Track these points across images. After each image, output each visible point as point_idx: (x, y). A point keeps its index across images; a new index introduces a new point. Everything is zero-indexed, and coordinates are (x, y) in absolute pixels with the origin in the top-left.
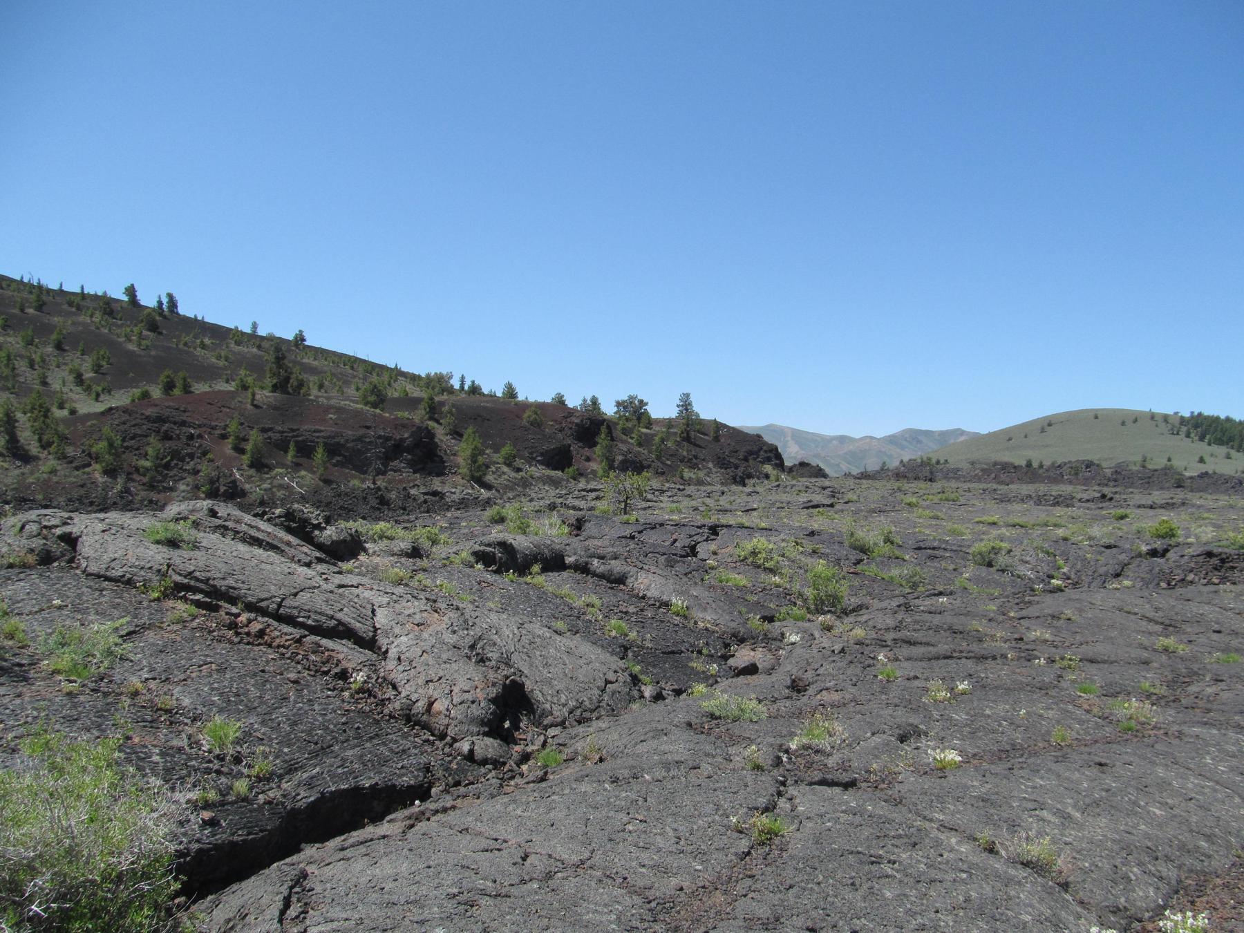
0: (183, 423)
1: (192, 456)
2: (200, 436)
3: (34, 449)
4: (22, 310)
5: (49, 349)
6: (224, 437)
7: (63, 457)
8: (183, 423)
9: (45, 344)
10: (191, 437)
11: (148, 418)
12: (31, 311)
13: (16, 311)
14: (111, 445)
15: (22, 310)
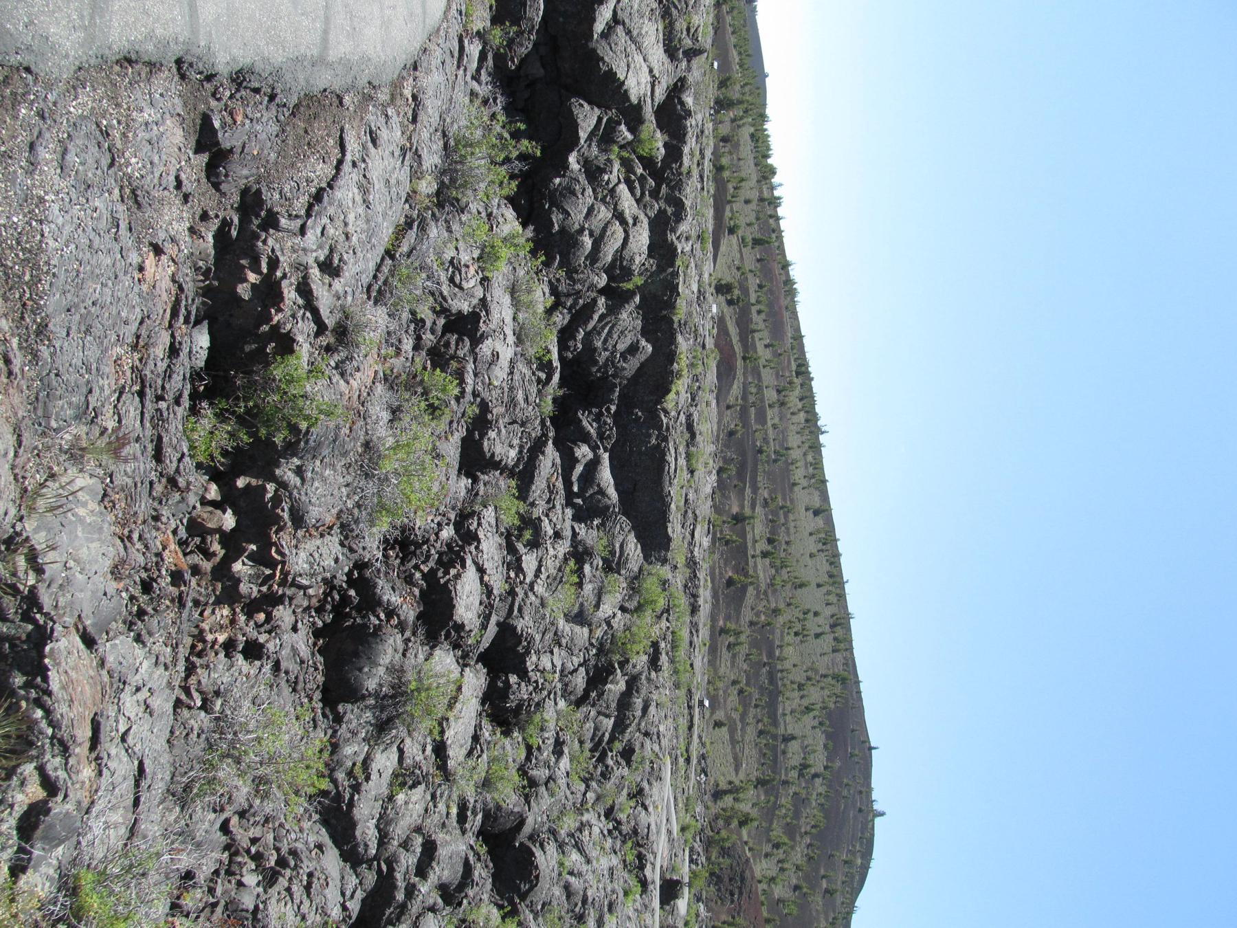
0: (741, 893)
1: (719, 890)
2: (732, 902)
3: (720, 804)
4: (823, 877)
5: (794, 881)
6: (733, 917)
7: (717, 817)
8: (741, 893)
9: (798, 879)
10: (732, 894)
11: (743, 872)
12: (825, 886)
13: (822, 872)
14: (723, 840)
15: (823, 877)
